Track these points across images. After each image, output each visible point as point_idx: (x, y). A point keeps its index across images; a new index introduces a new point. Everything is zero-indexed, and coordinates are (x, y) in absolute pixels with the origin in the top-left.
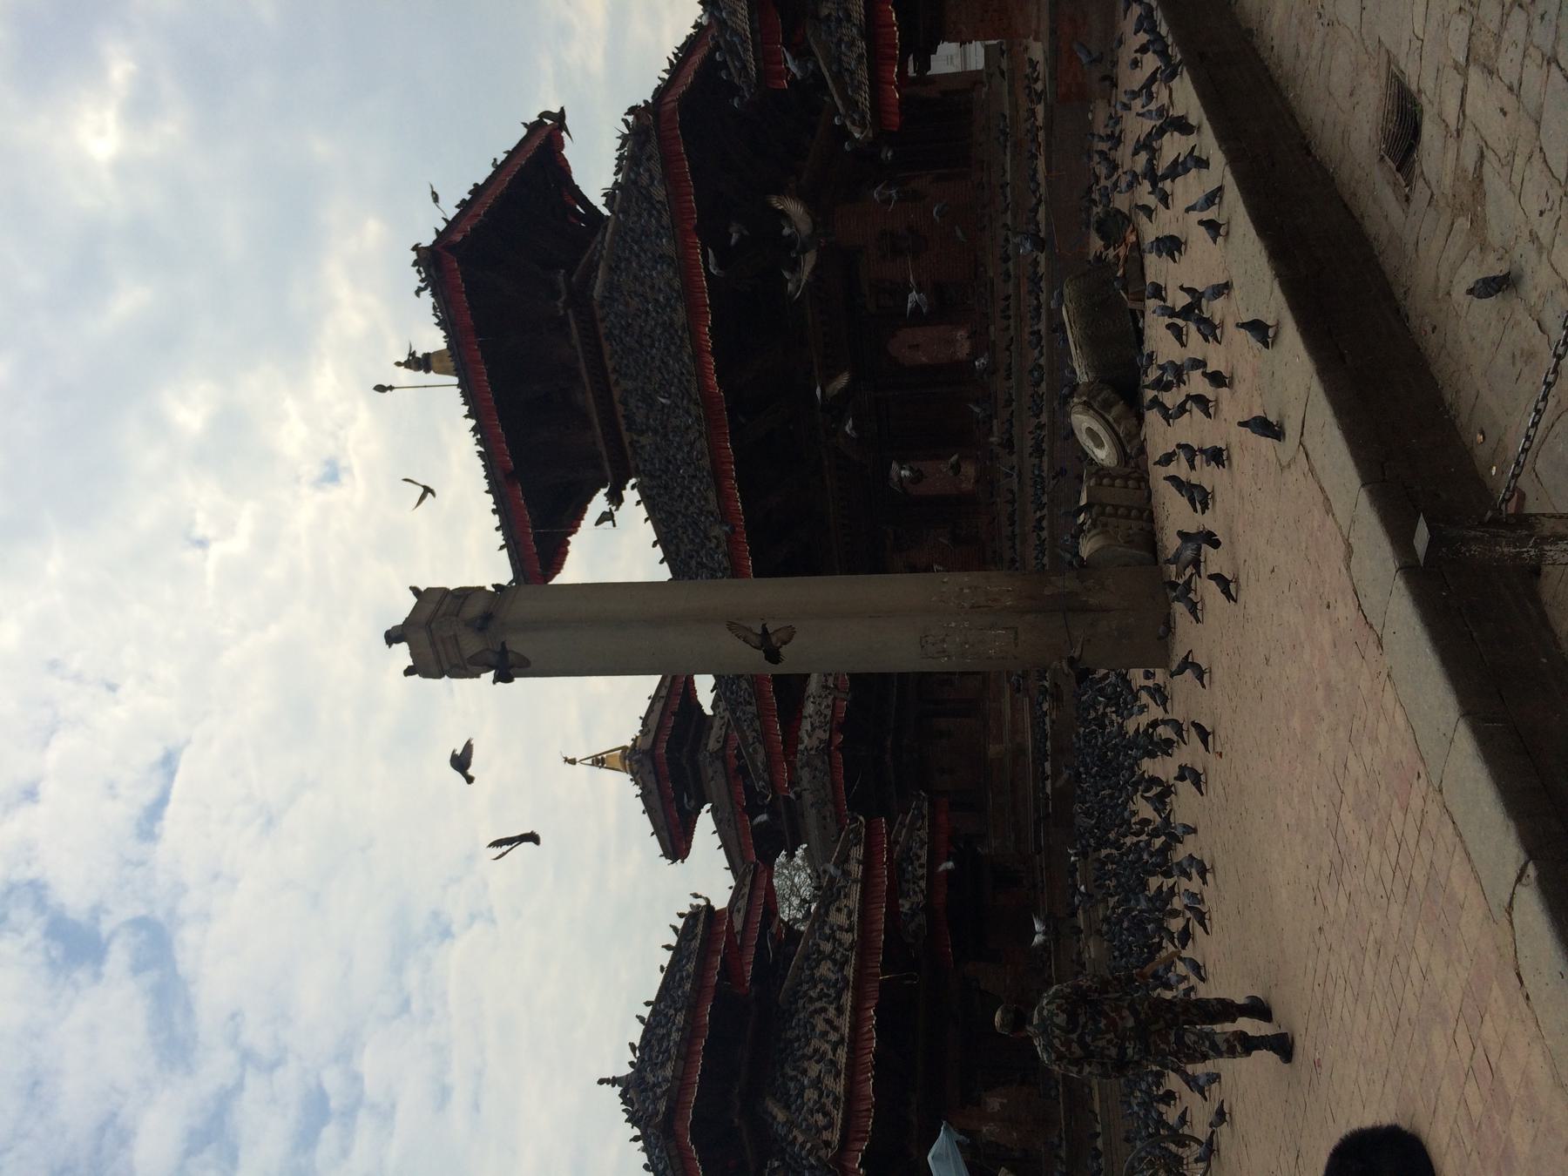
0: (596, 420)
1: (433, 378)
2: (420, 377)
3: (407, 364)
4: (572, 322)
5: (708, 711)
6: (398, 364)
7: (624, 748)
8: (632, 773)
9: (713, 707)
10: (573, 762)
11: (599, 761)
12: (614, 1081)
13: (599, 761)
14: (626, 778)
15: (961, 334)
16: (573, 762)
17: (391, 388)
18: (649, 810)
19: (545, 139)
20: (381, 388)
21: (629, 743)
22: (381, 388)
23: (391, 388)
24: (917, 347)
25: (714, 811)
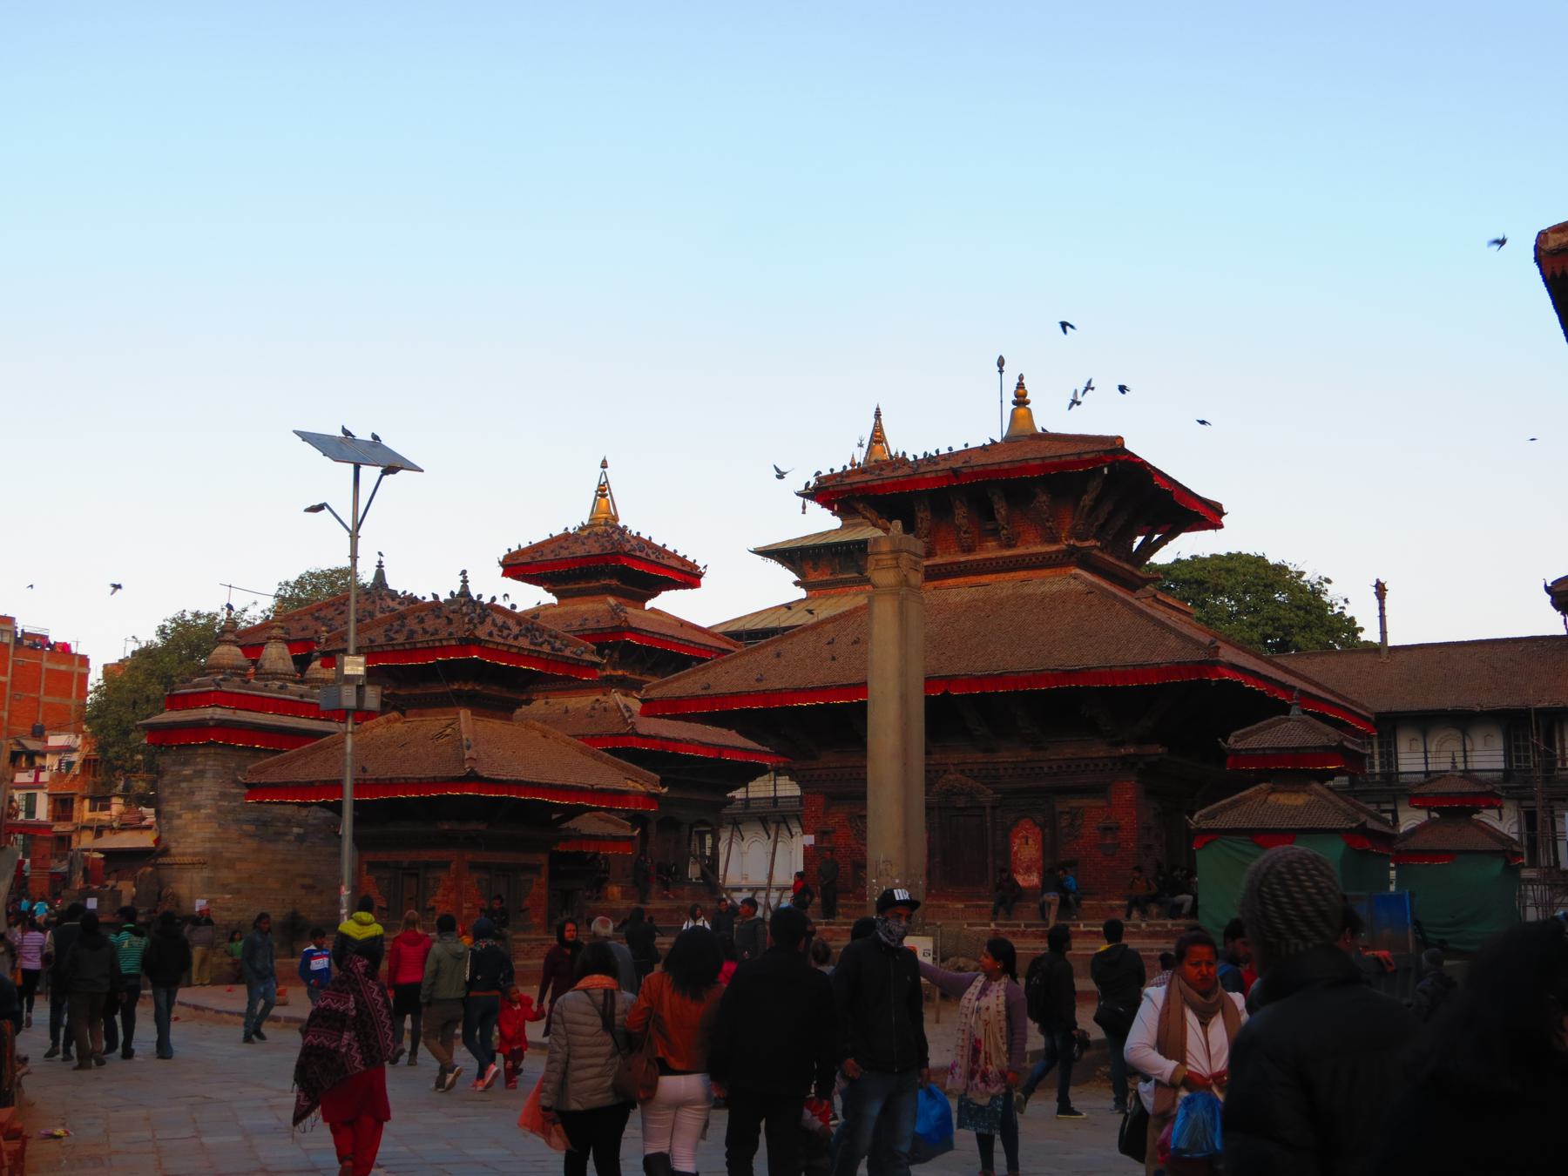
0: (970, 558)
1: (1009, 407)
2: (1010, 396)
3: (1020, 386)
4: (1054, 548)
5: (649, 604)
6: (1021, 378)
7: (616, 518)
8: (589, 526)
9: (652, 610)
10: (604, 465)
11: (603, 491)
12: (465, 582)
13: (603, 491)
14: (583, 517)
16: (604, 465)
17: (1001, 371)
18: (553, 540)
19: (1207, 515)
20: (1001, 363)
21: (621, 524)
22: (1001, 363)
23: (1001, 371)
25: (553, 605)
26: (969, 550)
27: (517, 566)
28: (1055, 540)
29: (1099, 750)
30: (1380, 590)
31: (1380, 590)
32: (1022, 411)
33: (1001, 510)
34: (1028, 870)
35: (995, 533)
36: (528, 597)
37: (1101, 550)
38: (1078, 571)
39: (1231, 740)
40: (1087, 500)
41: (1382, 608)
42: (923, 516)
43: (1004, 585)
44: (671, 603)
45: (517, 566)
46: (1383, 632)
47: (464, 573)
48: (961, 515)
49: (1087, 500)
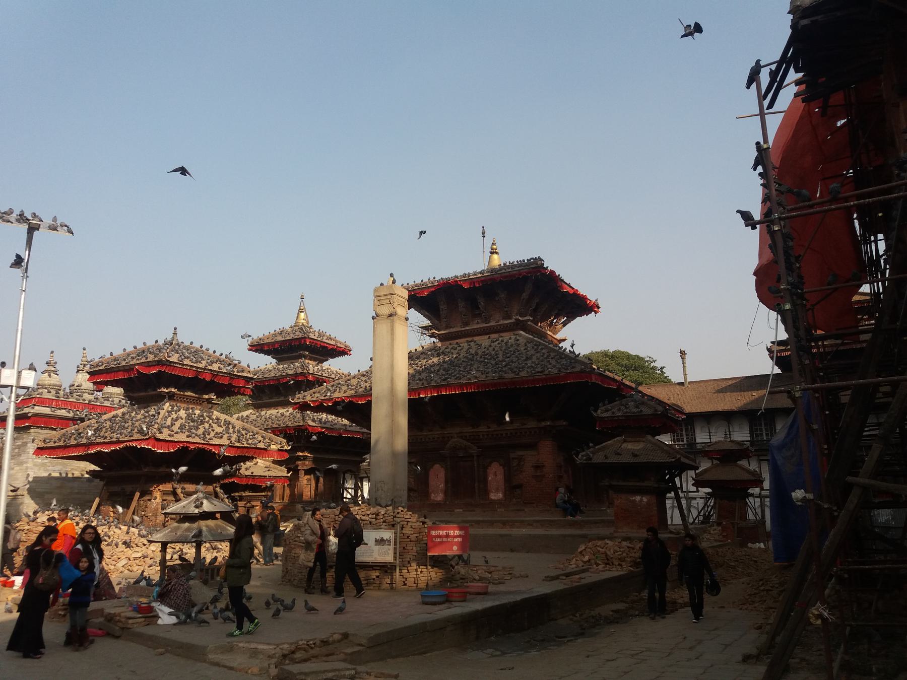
3: (493, 244)
15: (500, 495)
20: (483, 233)
24: (495, 475)
26: (467, 324)
27: (258, 347)
28: (510, 318)
29: (532, 424)
30: (683, 353)
31: (683, 353)
32: (495, 256)
33: (482, 303)
34: (497, 490)
35: (480, 315)
36: (263, 363)
37: (532, 321)
38: (522, 332)
39: (599, 411)
40: (525, 295)
41: (684, 363)
42: (443, 307)
43: (484, 341)
44: (334, 365)
45: (258, 347)
46: (685, 375)
47: (175, 329)
48: (461, 304)
49: (525, 295)
